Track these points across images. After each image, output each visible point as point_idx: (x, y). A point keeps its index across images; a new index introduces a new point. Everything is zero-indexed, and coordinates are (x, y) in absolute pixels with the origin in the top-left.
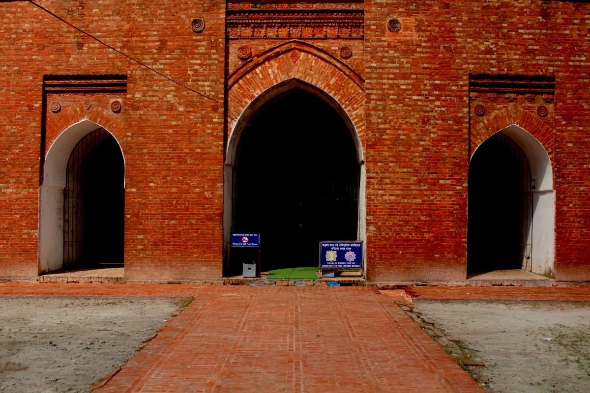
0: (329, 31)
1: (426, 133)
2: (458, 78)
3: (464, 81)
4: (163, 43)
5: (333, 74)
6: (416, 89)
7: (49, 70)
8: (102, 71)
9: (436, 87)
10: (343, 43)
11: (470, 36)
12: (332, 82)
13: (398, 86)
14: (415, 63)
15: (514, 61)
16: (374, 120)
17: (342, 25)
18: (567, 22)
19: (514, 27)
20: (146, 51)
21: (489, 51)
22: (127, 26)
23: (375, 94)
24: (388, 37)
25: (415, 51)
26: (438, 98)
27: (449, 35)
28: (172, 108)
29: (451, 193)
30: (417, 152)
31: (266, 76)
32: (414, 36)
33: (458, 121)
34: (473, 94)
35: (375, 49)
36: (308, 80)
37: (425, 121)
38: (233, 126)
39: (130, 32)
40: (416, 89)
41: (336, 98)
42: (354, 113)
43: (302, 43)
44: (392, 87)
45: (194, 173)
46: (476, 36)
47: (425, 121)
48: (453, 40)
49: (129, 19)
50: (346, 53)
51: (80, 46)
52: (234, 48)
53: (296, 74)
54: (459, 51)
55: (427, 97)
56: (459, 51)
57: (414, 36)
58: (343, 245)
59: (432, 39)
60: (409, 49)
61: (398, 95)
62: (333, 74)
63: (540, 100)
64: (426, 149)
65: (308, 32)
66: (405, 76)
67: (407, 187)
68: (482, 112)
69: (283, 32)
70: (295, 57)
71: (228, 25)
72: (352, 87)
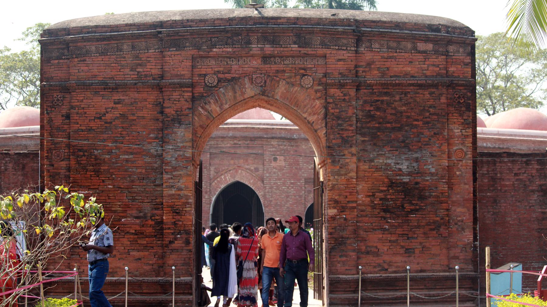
1: (288, 201)
2: (300, 180)
3: (303, 181)
5: (252, 178)
6: (284, 184)
9: (292, 183)
10: (255, 166)
11: (305, 163)
12: (252, 181)
13: (277, 183)
14: (283, 175)
16: (268, 196)
23: (268, 186)
24: (273, 164)
25: (283, 170)
26: (292, 187)
27: (297, 163)
31: (226, 179)
32: (283, 164)
33: (300, 196)
34: (306, 186)
35: (268, 169)
36: (242, 181)
38: (213, 199)
40: (284, 184)
41: (253, 188)
42: (260, 194)
44: (275, 184)
47: (287, 197)
48: (298, 165)
53: (237, 179)
54: (300, 169)
55: (288, 187)
56: (300, 169)
57: (283, 164)
59: (290, 165)
60: (281, 169)
61: (277, 187)
62: (252, 178)
64: (288, 208)
66: (279, 179)
70: (237, 172)
71: (210, 158)
72: (259, 183)
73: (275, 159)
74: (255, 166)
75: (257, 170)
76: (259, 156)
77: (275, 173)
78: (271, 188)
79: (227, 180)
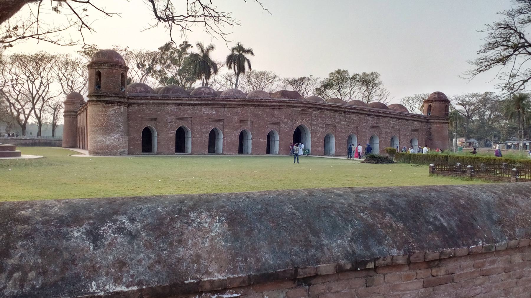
15: (330, 123)
68: (326, 130)
79: (299, 123)
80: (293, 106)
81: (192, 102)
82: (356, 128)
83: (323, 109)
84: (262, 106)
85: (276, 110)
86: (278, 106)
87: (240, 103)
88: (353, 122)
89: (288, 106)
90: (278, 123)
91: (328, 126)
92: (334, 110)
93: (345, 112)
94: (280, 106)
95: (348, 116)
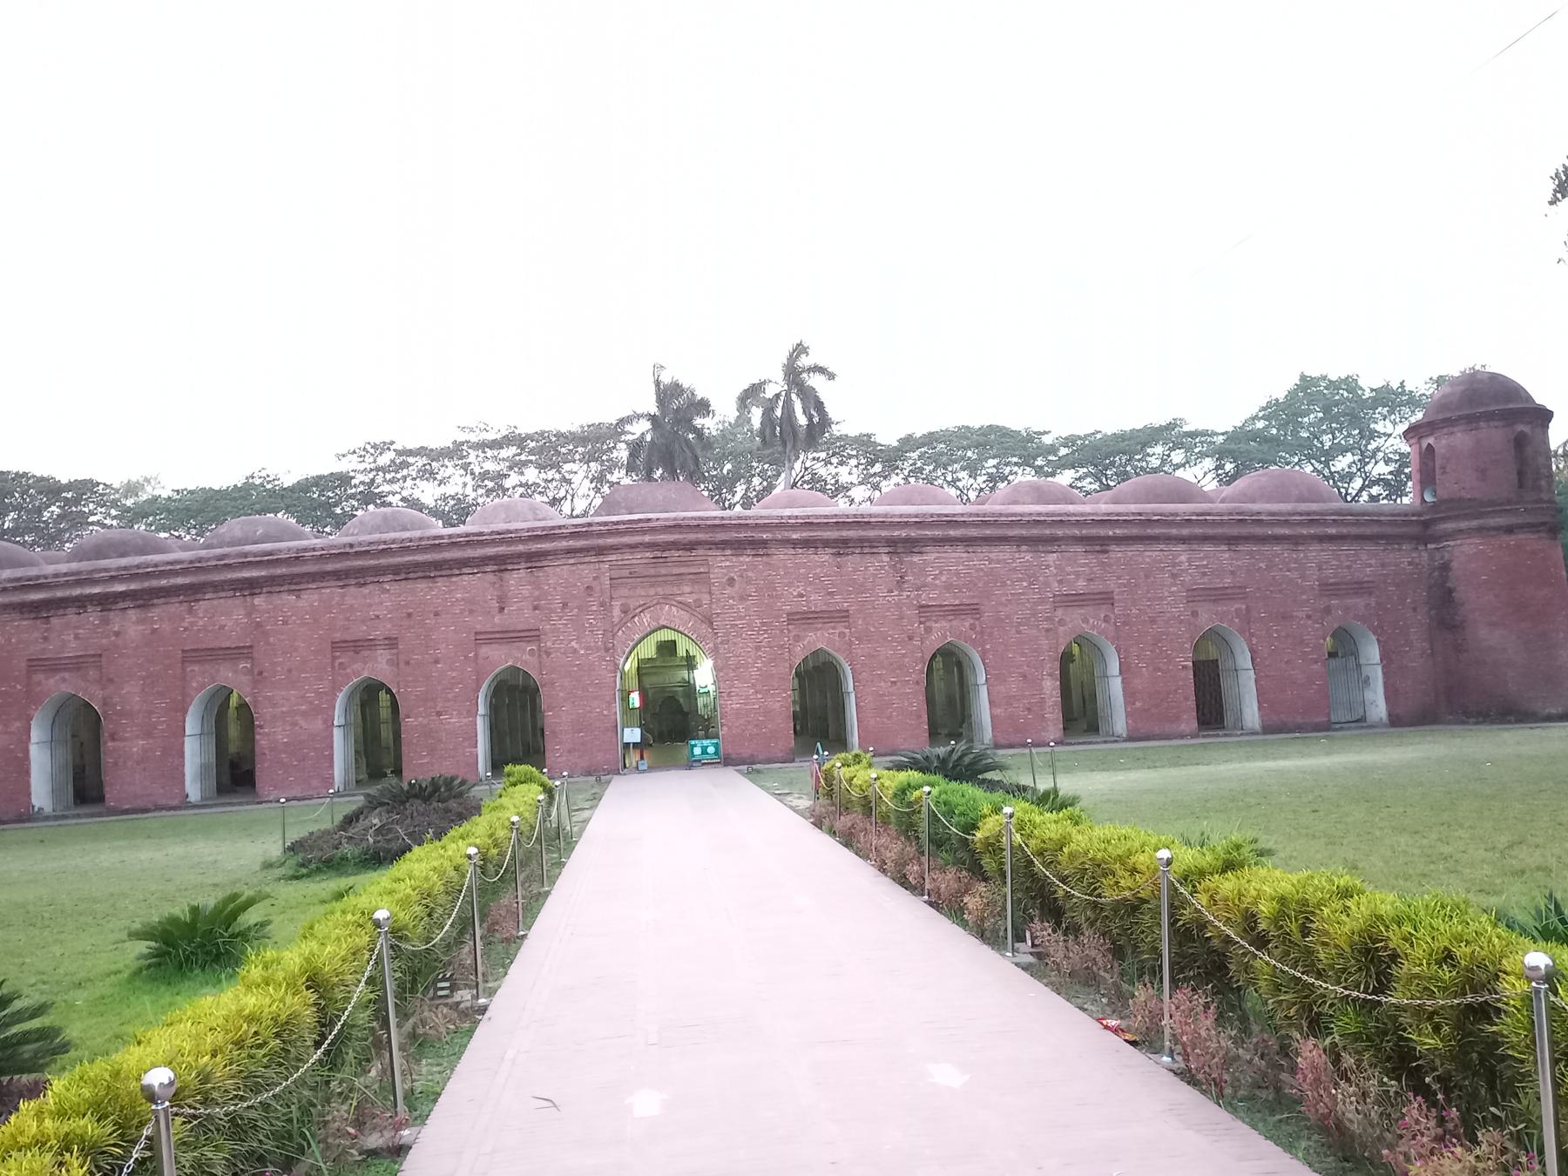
0: (687, 589)
4: (565, 605)
6: (750, 626)
7: (479, 627)
8: (520, 627)
9: (763, 624)
10: (695, 596)
15: (817, 601)
17: (694, 582)
18: (855, 570)
19: (817, 577)
20: (552, 611)
21: (801, 595)
22: (537, 593)
28: (575, 651)
29: (782, 701)
30: (754, 672)
37: (758, 648)
39: (538, 598)
43: (667, 598)
45: (595, 698)
46: (790, 585)
47: (758, 648)
49: (538, 588)
50: (698, 603)
51: (502, 609)
52: (617, 604)
56: (779, 597)
58: (706, 742)
63: (841, 628)
64: (759, 669)
65: (668, 590)
66: (741, 618)
67: (747, 697)
68: (797, 638)
69: (652, 591)
73: (731, 581)
74: (695, 596)
75: (698, 603)
76: (701, 579)
77: (731, 607)
78: (727, 634)
80: (601, 551)
81: (96, 590)
82: (974, 610)
83: (764, 543)
84: (437, 565)
85: (517, 579)
86: (520, 555)
87: (329, 567)
88: (948, 587)
89: (570, 552)
90: (531, 635)
91: (806, 618)
92: (826, 543)
93: (892, 543)
94: (530, 557)
95: (916, 559)
